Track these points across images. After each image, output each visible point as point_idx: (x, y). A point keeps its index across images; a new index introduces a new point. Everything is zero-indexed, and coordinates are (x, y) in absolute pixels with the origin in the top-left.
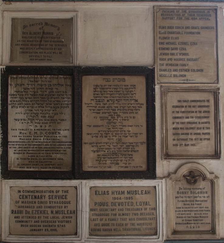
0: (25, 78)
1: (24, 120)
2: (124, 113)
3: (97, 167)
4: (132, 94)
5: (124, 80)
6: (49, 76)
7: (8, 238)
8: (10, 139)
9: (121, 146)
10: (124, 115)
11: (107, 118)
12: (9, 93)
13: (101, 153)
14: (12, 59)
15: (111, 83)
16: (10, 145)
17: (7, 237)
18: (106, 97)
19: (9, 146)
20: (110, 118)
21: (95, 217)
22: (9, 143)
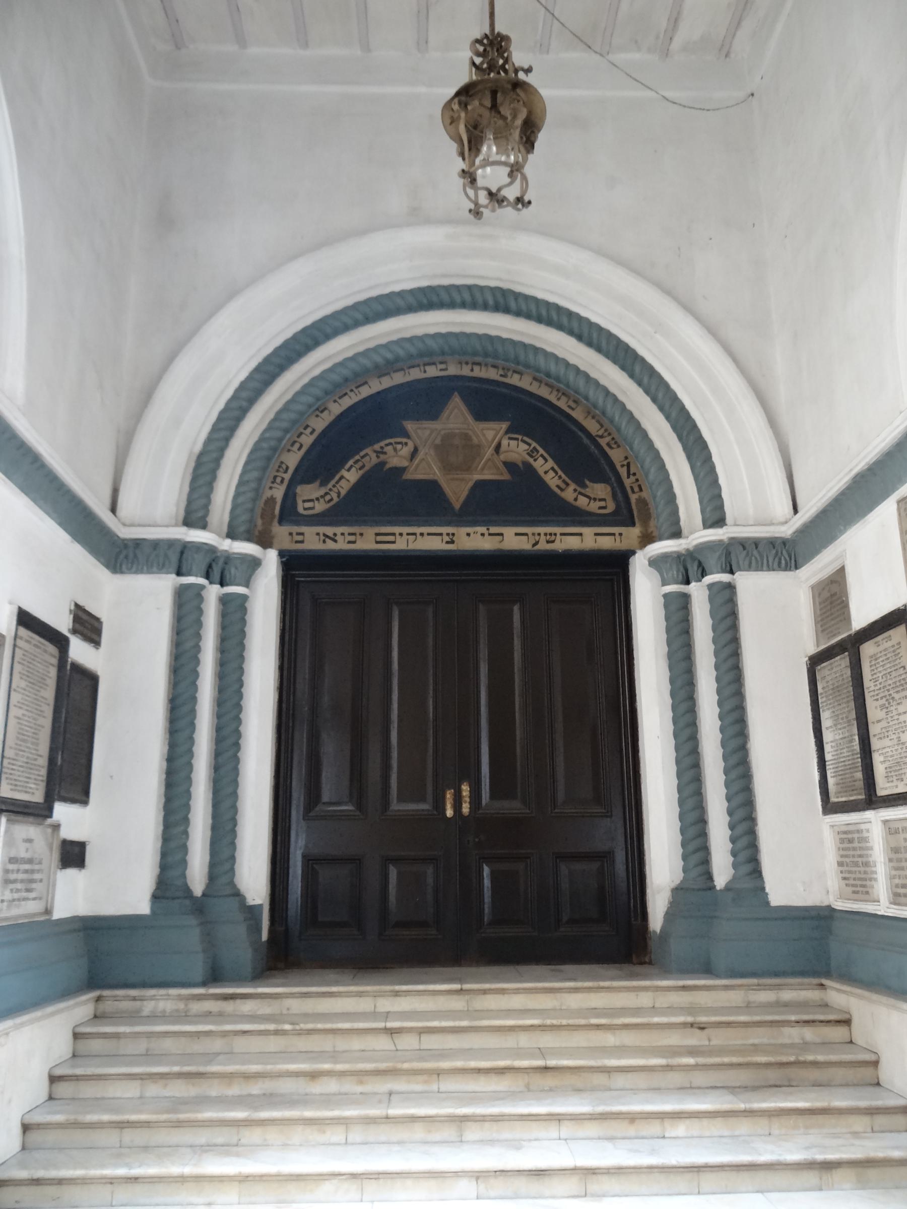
0: (824, 667)
1: (831, 727)
2: (897, 692)
3: (886, 789)
4: (900, 658)
5: (889, 638)
6: (839, 657)
7: (836, 903)
8: (828, 757)
9: (902, 748)
10: (897, 696)
11: (885, 704)
12: (819, 692)
13: (887, 764)
14: (818, 646)
15: (881, 648)
16: (829, 765)
17: (836, 901)
18: (880, 672)
19: (827, 768)
20: (887, 705)
21: (894, 872)
22: (827, 763)
